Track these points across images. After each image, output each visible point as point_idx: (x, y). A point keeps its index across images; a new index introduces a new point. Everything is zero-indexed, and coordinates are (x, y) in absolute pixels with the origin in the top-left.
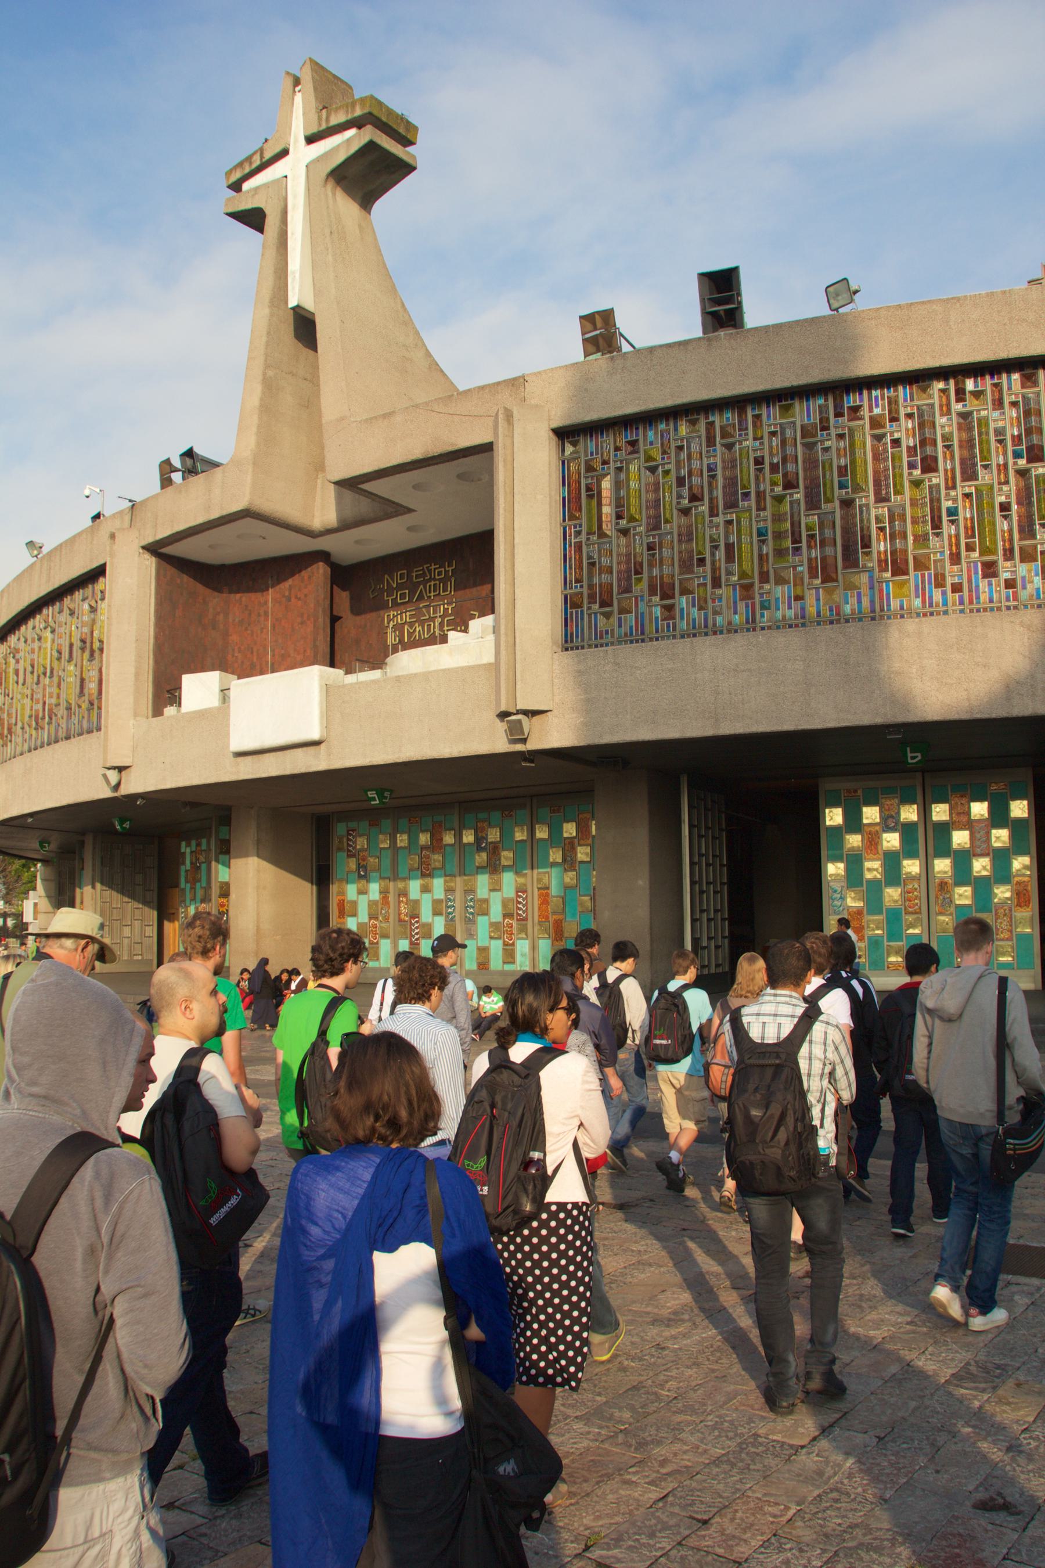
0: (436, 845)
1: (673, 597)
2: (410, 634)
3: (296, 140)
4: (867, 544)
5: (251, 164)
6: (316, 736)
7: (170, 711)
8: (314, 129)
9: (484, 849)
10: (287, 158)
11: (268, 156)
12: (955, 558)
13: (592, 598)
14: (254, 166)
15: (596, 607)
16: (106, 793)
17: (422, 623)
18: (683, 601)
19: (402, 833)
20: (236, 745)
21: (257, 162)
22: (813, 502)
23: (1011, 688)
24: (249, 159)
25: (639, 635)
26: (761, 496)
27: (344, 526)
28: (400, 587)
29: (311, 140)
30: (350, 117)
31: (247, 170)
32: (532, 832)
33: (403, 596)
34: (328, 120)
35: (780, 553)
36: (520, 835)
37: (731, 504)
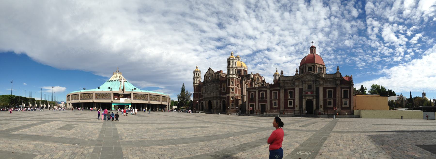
25: (135, 100)
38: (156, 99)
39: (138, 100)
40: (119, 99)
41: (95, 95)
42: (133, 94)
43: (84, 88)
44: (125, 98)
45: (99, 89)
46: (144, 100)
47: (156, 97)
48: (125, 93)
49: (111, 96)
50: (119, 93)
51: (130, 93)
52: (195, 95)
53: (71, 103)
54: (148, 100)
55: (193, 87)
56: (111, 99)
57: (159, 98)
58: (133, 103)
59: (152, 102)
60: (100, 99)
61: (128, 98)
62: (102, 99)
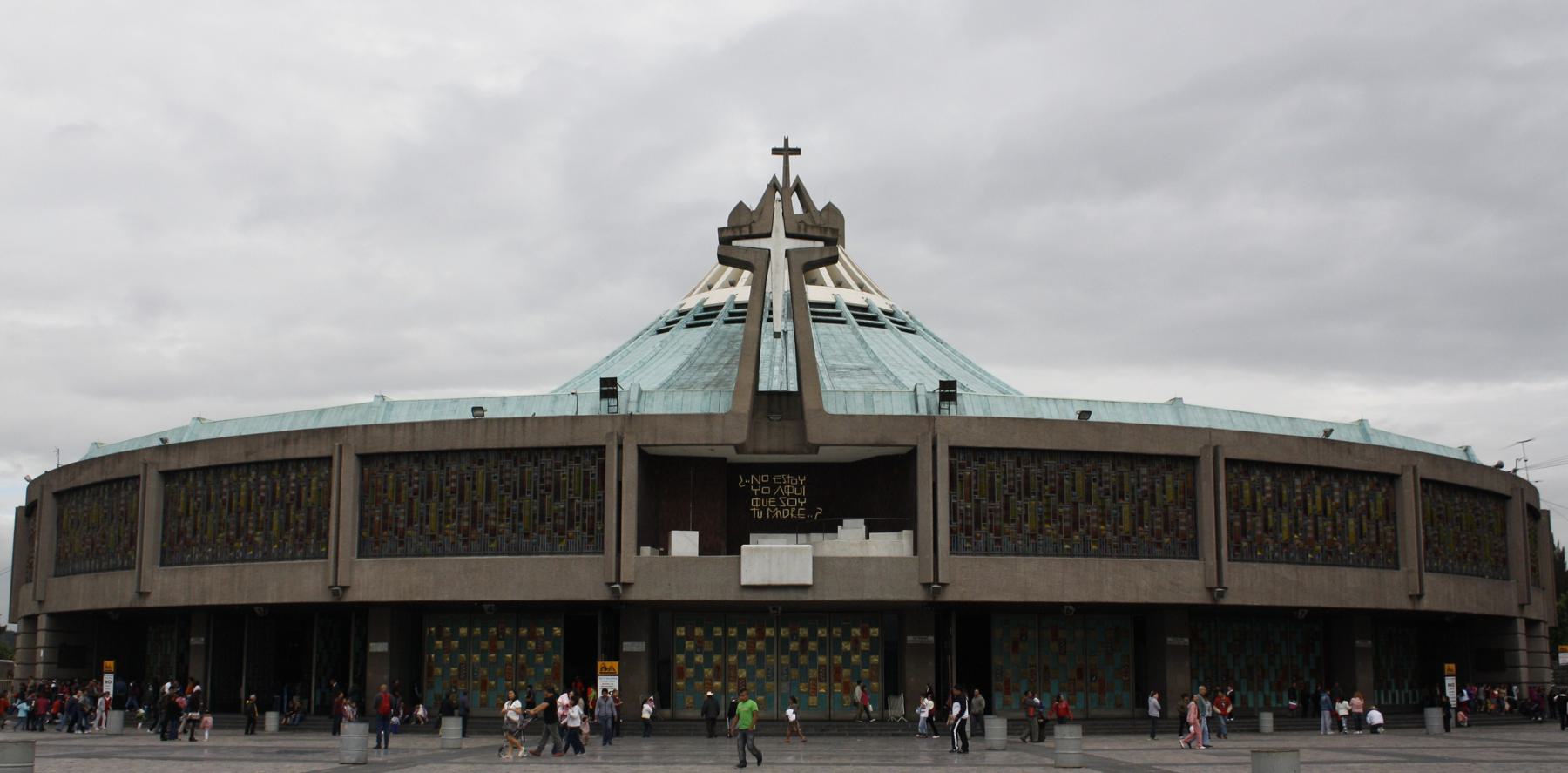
1: (1000, 535)
2: (771, 516)
3: (777, 231)
5: (741, 231)
6: (810, 582)
7: (646, 551)
8: (794, 231)
9: (796, 640)
10: (768, 239)
11: (755, 232)
12: (1115, 534)
13: (962, 530)
14: (744, 234)
15: (963, 535)
17: (781, 509)
18: (1004, 538)
19: (733, 627)
20: (744, 581)
21: (746, 232)
22: (1061, 498)
24: (740, 227)
25: (987, 551)
26: (1040, 494)
28: (765, 484)
29: (788, 235)
30: (823, 235)
31: (738, 234)
33: (766, 490)
34: (805, 230)
35: (1048, 522)
36: (821, 633)
38: (1326, 525)
39: (1034, 546)
41: (365, 490)
42: (953, 451)
44: (831, 528)
46: (1126, 547)
47: (1328, 492)
48: (825, 455)
49: (601, 505)
50: (730, 454)
53: (43, 622)
54: (1189, 548)
56: (600, 549)
58: (951, 596)
61: (871, 528)
62: (467, 543)
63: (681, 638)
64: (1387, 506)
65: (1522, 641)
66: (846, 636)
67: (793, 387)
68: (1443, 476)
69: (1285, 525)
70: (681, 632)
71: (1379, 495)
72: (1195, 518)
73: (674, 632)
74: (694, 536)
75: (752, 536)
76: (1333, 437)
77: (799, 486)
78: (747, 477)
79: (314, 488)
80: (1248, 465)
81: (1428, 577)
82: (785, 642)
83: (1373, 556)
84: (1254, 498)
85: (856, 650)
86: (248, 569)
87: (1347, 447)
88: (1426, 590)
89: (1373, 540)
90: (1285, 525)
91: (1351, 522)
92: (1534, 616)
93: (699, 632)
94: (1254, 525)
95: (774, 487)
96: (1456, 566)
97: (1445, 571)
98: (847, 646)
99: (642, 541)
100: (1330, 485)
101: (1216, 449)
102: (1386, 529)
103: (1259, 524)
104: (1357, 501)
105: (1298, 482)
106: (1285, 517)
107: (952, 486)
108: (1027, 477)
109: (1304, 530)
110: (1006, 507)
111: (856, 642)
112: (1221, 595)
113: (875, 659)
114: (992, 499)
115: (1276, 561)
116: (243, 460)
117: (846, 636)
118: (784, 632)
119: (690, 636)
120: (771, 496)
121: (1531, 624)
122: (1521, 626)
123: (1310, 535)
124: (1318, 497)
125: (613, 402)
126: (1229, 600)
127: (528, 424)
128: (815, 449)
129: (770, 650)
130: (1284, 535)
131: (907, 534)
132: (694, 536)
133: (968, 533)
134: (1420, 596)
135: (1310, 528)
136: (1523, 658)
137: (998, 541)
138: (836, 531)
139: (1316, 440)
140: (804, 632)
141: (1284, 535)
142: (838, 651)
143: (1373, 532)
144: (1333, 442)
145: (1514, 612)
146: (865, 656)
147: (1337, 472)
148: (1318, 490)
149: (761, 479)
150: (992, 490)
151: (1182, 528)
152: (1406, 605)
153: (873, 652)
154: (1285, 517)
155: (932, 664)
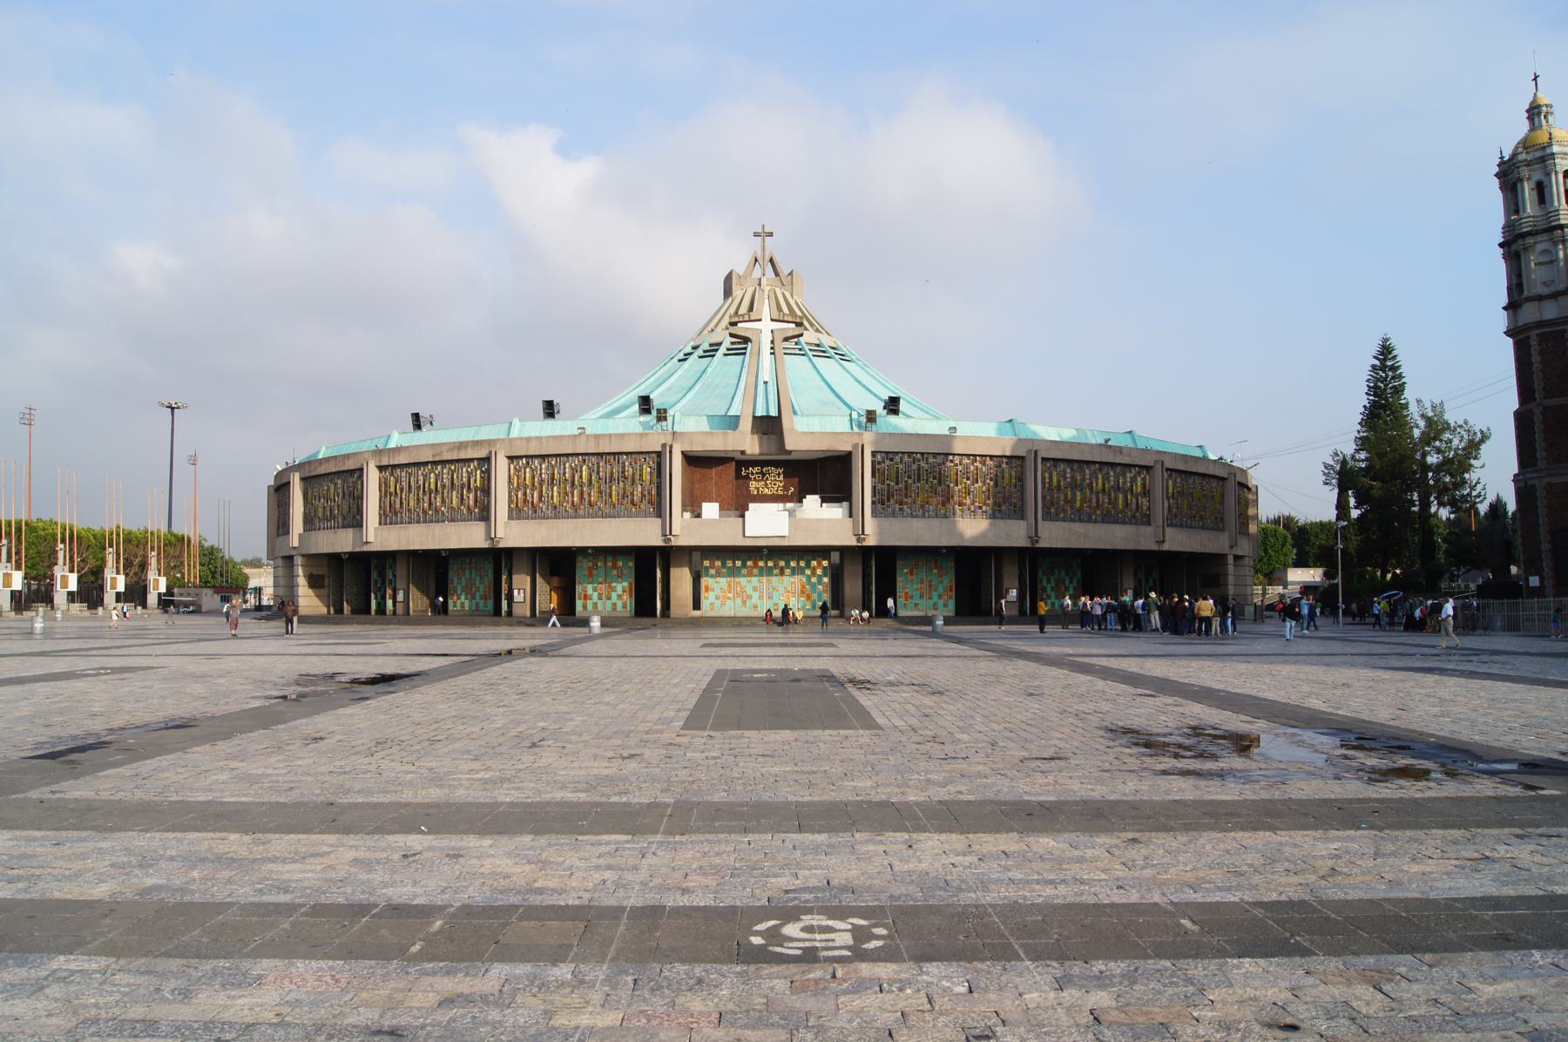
0: (756, 565)
4: (953, 497)
11: (752, 318)
16: (662, 544)
18: (905, 507)
22: (940, 484)
23: (976, 538)
25: (893, 515)
27: (760, 454)
29: (772, 320)
32: (798, 564)
36: (793, 564)
37: (919, 481)
40: (738, 506)
43: (416, 417)
45: (550, 422)
47: (1106, 478)
51: (848, 448)
52: (1538, 437)
55: (1510, 341)
57: (1138, 488)
59: (1057, 535)
60: (557, 513)
61: (824, 500)
63: (707, 567)
64: (1144, 486)
65: (1231, 569)
66: (808, 565)
67: (774, 413)
68: (1181, 467)
69: (1078, 498)
70: (707, 563)
71: (1139, 479)
72: (1022, 494)
73: (702, 563)
74: (716, 505)
75: (751, 505)
76: (1109, 443)
77: (779, 474)
78: (747, 469)
79: (478, 477)
80: (1056, 461)
81: (1169, 531)
82: (770, 569)
83: (1134, 517)
84: (1059, 482)
85: (814, 573)
86: (437, 528)
87: (1119, 450)
88: (1167, 538)
89: (1134, 507)
90: (1078, 498)
91: (1121, 496)
92: (1240, 553)
93: (718, 563)
94: (1058, 498)
95: (764, 475)
96: (1189, 523)
97: (1181, 526)
98: (808, 572)
99: (684, 509)
100: (1108, 473)
101: (1036, 452)
102: (1144, 502)
103: (1062, 497)
104: (1125, 483)
105: (1087, 472)
106: (1078, 494)
107: (873, 475)
108: (919, 470)
109: (1090, 500)
110: (906, 489)
111: (814, 569)
112: (1037, 541)
113: (826, 580)
114: (897, 483)
115: (1072, 520)
116: (431, 460)
117: (808, 565)
118: (770, 564)
119: (712, 566)
120: (762, 480)
121: (1237, 558)
122: (1231, 560)
123: (1094, 504)
124: (1100, 481)
125: (664, 423)
126: (1042, 544)
127: (613, 438)
128: (790, 452)
129: (761, 575)
130: (1078, 504)
131: (845, 504)
132: (716, 505)
133: (883, 504)
134: (1163, 541)
135: (1094, 500)
136: (1231, 579)
137: (901, 509)
138: (801, 502)
139: (1101, 445)
140: (782, 563)
141: (1078, 504)
142: (803, 573)
143: (1134, 500)
144: (1110, 447)
145: (1226, 551)
146: (820, 578)
147: (1113, 465)
148: (1100, 476)
149: (756, 470)
150: (897, 478)
151: (1014, 501)
152: (1154, 547)
153: (825, 575)
154: (1078, 494)
155: (860, 583)
